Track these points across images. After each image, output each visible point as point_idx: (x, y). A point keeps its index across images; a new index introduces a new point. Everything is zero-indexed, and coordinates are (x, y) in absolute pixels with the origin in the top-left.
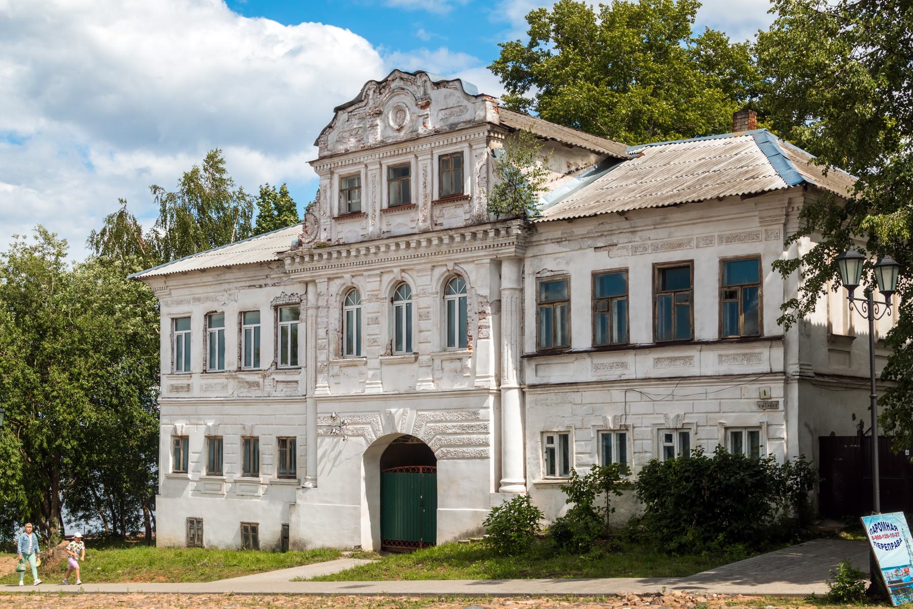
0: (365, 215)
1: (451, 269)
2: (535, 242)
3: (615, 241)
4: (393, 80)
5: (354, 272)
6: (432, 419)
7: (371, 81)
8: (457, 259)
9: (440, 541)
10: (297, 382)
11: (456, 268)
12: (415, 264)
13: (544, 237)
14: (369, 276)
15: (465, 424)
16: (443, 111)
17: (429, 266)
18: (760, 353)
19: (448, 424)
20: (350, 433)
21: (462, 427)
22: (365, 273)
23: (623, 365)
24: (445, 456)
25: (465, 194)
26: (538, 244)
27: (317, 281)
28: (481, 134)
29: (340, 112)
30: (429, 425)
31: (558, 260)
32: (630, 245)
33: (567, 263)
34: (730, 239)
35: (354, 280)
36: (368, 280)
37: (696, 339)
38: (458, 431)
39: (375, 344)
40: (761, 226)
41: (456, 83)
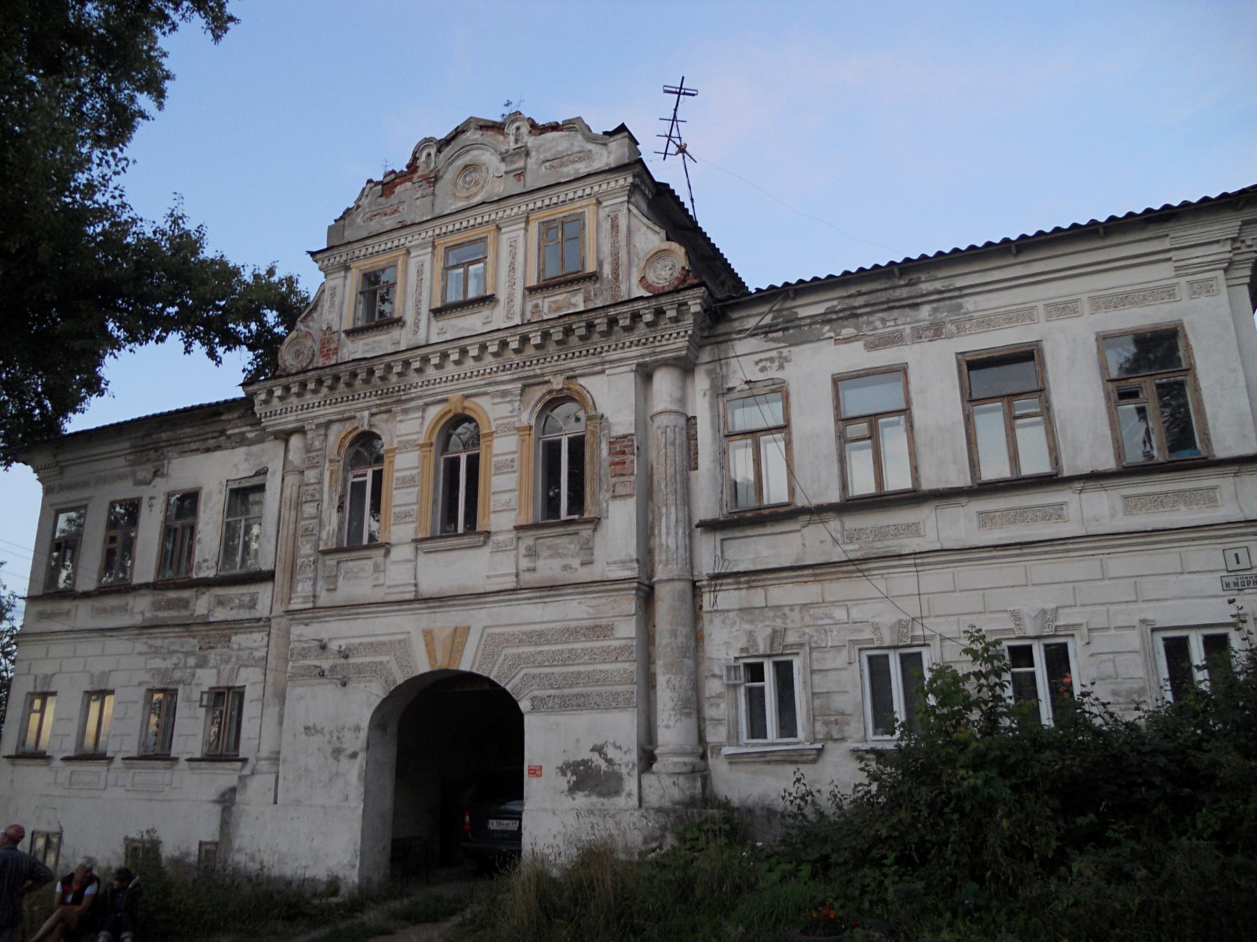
2: (718, 335)
8: (571, 369)
13: (737, 325)
18: (1214, 488)
26: (727, 339)
27: (307, 428)
28: (621, 182)
31: (761, 365)
33: (781, 367)
34: (1124, 299)
37: (1066, 473)
40: (1177, 276)
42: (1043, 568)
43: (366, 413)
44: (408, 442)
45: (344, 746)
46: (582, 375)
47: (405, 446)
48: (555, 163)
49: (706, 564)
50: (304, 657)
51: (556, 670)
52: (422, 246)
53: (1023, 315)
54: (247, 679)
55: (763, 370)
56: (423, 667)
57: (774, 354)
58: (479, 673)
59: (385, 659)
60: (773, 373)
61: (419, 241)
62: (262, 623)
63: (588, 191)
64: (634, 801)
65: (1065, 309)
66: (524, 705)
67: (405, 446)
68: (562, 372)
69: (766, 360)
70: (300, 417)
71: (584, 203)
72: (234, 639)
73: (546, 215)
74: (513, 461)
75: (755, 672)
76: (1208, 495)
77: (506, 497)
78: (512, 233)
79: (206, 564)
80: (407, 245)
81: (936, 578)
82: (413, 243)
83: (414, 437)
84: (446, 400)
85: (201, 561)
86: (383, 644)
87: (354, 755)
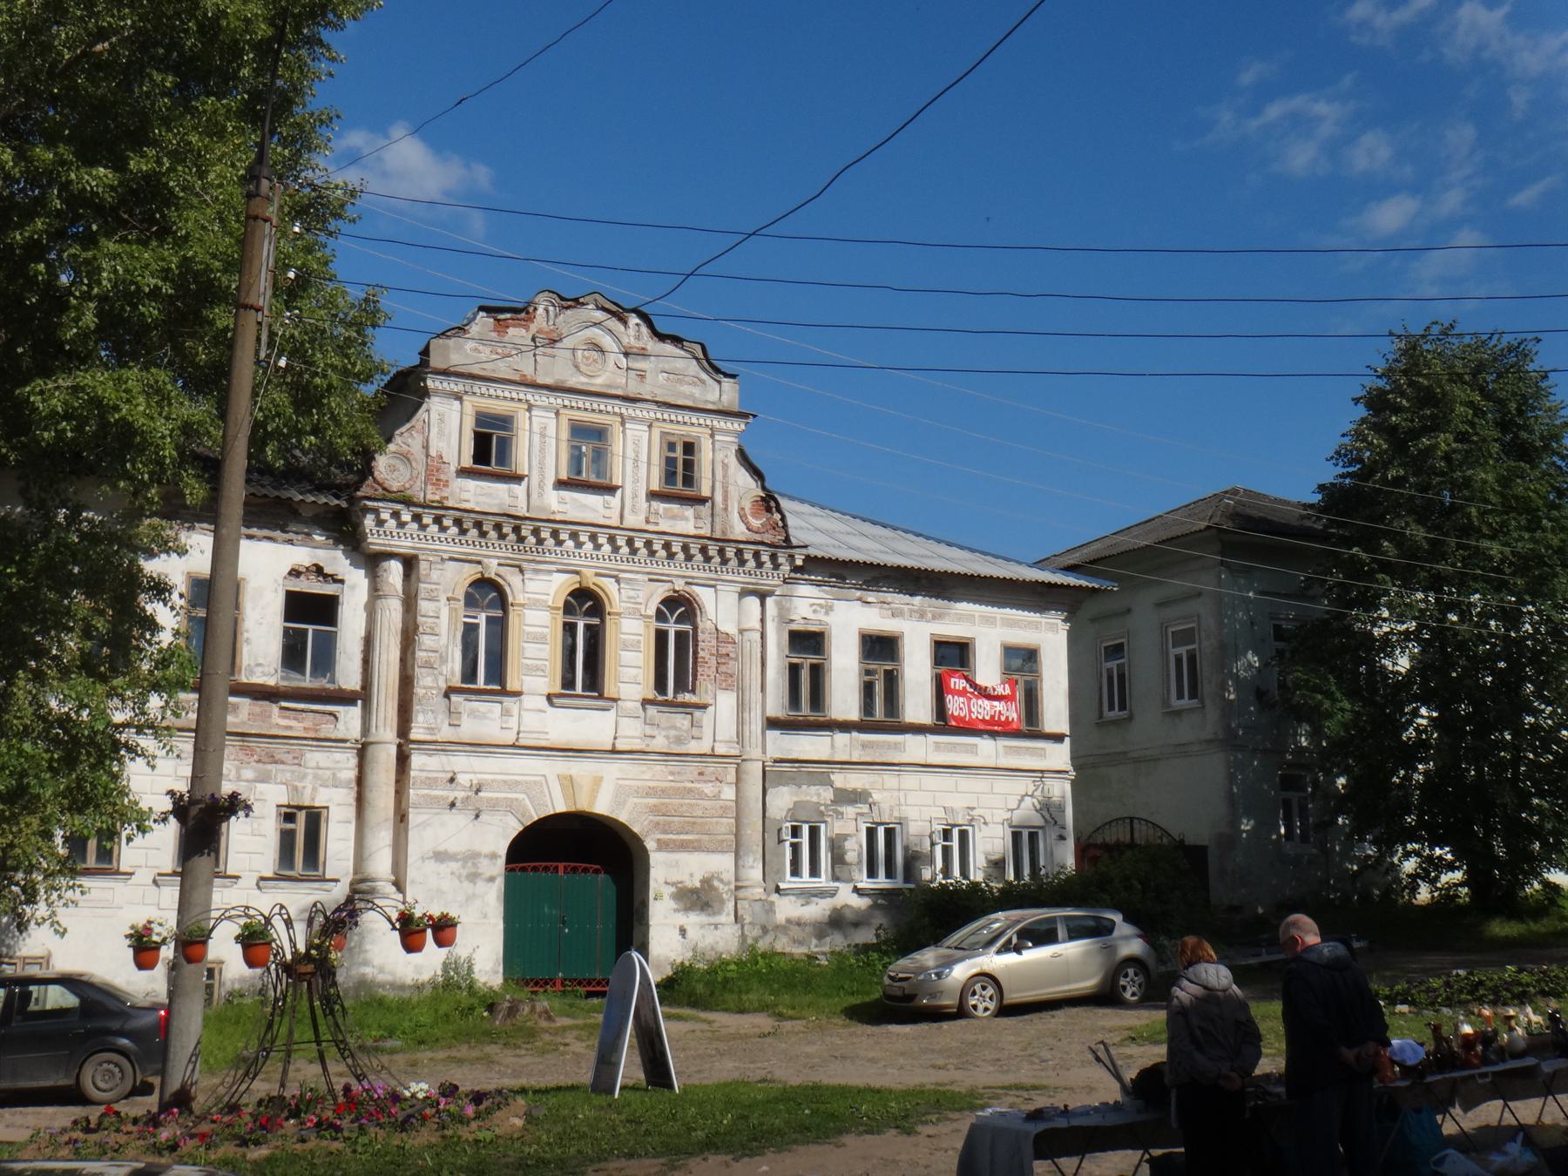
3: (889, 600)
23: (896, 746)
27: (421, 557)
32: (906, 607)
33: (827, 613)
35: (503, 570)
39: (539, 673)
42: (964, 782)
43: (496, 562)
44: (538, 600)
45: (480, 871)
47: (536, 605)
48: (671, 376)
49: (773, 752)
50: (430, 787)
51: (676, 819)
53: (970, 618)
54: (330, 800)
55: (815, 611)
56: (561, 807)
57: (822, 602)
58: (613, 816)
59: (521, 796)
60: (821, 616)
61: (546, 404)
62: (348, 745)
64: (732, 918)
65: (989, 621)
66: (650, 845)
67: (536, 605)
68: (684, 577)
71: (700, 429)
72: (308, 755)
73: (669, 427)
74: (639, 642)
75: (795, 832)
76: (1042, 754)
77: (633, 671)
78: (637, 432)
79: (260, 669)
80: (532, 402)
81: (910, 780)
82: (539, 403)
83: (544, 597)
84: (577, 573)
85: (252, 664)
86: (517, 783)
87: (492, 879)
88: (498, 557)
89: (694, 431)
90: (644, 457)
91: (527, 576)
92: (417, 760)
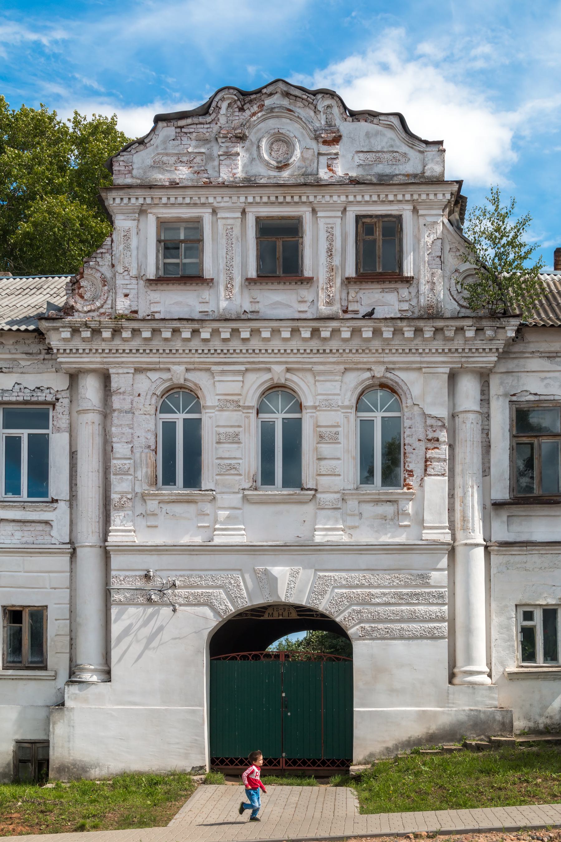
0: (209, 283)
1: (378, 375)
2: (515, 353)
4: (271, 94)
5: (190, 363)
6: (344, 583)
7: (229, 88)
8: (394, 363)
9: (359, 754)
10: (47, 523)
11: (388, 375)
12: (315, 363)
13: (532, 347)
14: (223, 372)
15: (405, 591)
16: (361, 155)
17: (342, 367)
19: (373, 591)
20: (181, 601)
21: (400, 596)
22: (214, 368)
24: (366, 635)
25: (405, 274)
26: (521, 355)
27: (111, 371)
28: (440, 196)
29: (160, 124)
30: (336, 590)
36: (217, 378)
38: (393, 600)
39: (233, 472)
41: (392, 118)
43: (182, 368)
46: (400, 369)
52: (230, 209)
61: (229, 204)
63: (408, 197)
69: (550, 378)
70: (105, 360)
71: (400, 206)
80: (216, 204)
82: (222, 205)
88: (186, 363)
89: (392, 209)
90: (338, 244)
91: (217, 378)
92: (116, 561)
